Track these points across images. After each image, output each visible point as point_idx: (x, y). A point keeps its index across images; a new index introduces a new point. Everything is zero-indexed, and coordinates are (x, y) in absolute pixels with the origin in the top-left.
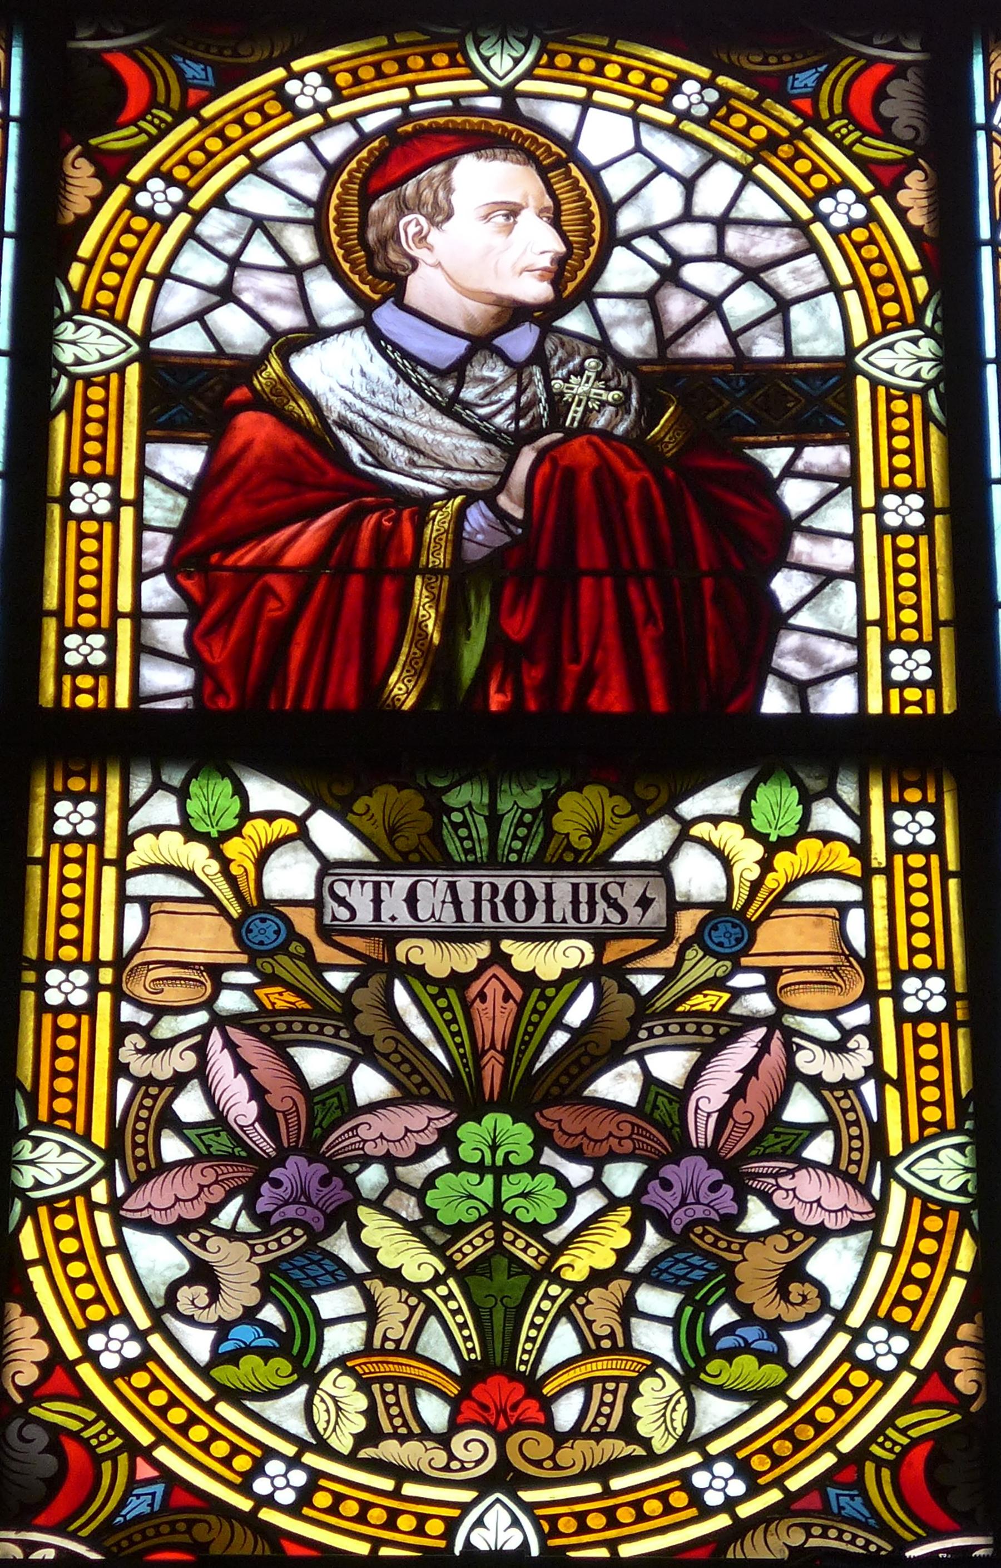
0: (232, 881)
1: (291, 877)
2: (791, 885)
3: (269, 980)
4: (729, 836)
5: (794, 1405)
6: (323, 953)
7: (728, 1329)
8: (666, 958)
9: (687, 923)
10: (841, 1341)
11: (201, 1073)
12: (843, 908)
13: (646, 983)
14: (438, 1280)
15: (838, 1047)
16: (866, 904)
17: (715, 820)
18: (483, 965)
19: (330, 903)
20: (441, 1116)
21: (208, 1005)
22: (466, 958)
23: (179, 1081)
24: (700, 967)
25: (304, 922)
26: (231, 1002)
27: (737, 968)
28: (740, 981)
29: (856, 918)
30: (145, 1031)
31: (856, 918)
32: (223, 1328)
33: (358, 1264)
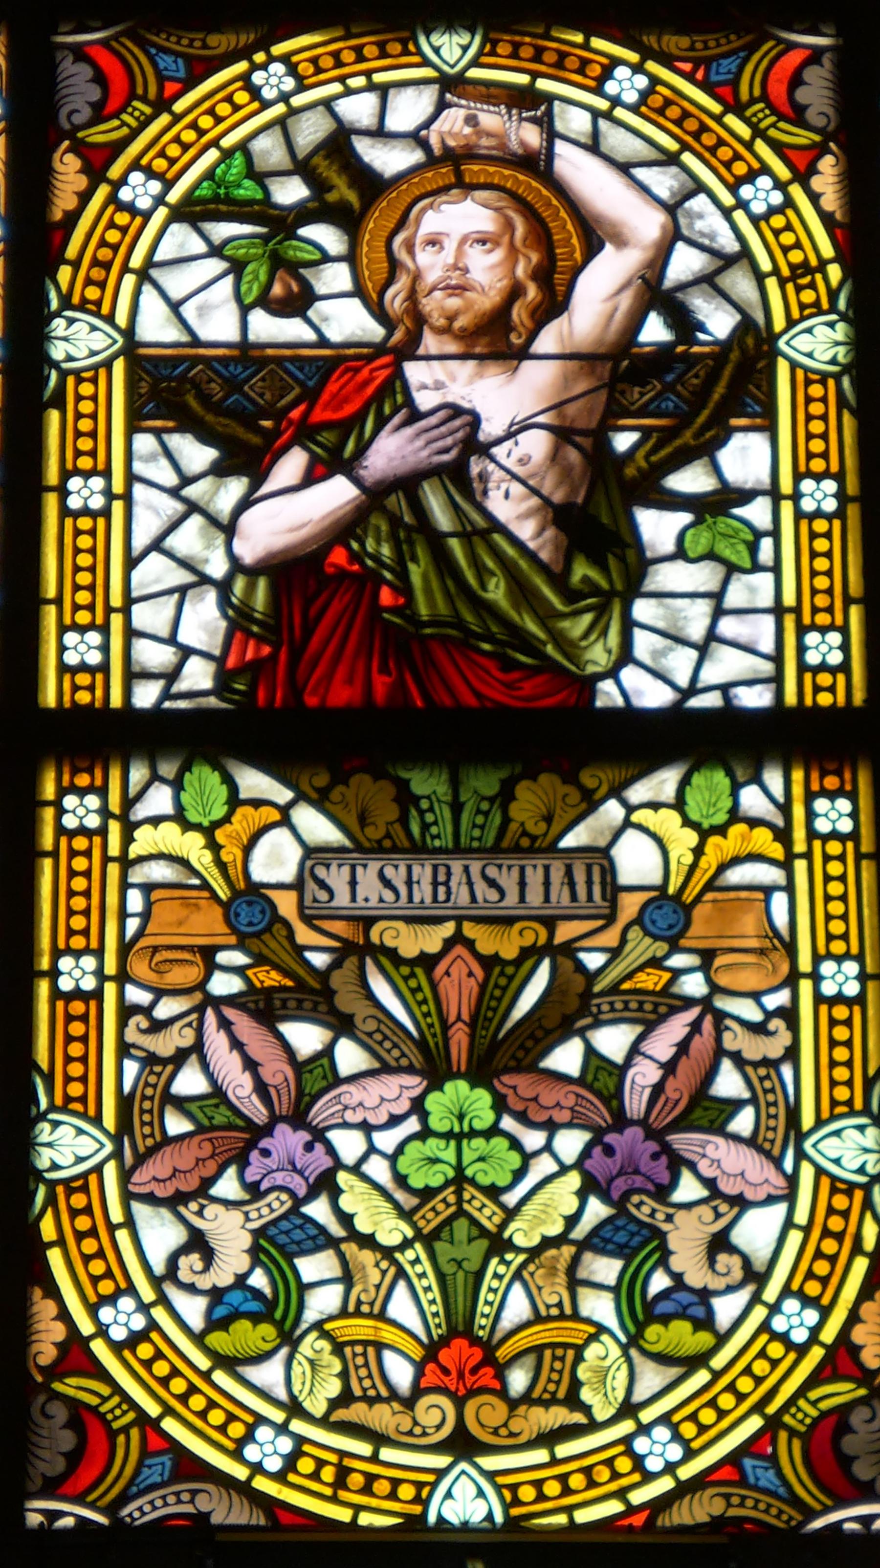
0: (222, 866)
1: (275, 861)
2: (722, 868)
3: (260, 960)
4: (667, 822)
5: (717, 1375)
6: (304, 935)
7: (664, 1295)
8: (610, 938)
9: (630, 905)
10: (759, 1313)
11: (198, 1047)
12: (768, 891)
13: (593, 961)
14: (406, 1244)
15: (759, 1029)
16: (790, 888)
17: (655, 806)
18: (449, 944)
19: (311, 886)
20: (414, 1084)
21: (202, 986)
22: (431, 939)
23: (179, 1058)
24: (642, 946)
25: (286, 904)
26: (223, 984)
27: (675, 948)
28: (678, 961)
29: (779, 901)
30: (147, 1011)
31: (779, 901)
32: (216, 1295)
33: (336, 1230)
